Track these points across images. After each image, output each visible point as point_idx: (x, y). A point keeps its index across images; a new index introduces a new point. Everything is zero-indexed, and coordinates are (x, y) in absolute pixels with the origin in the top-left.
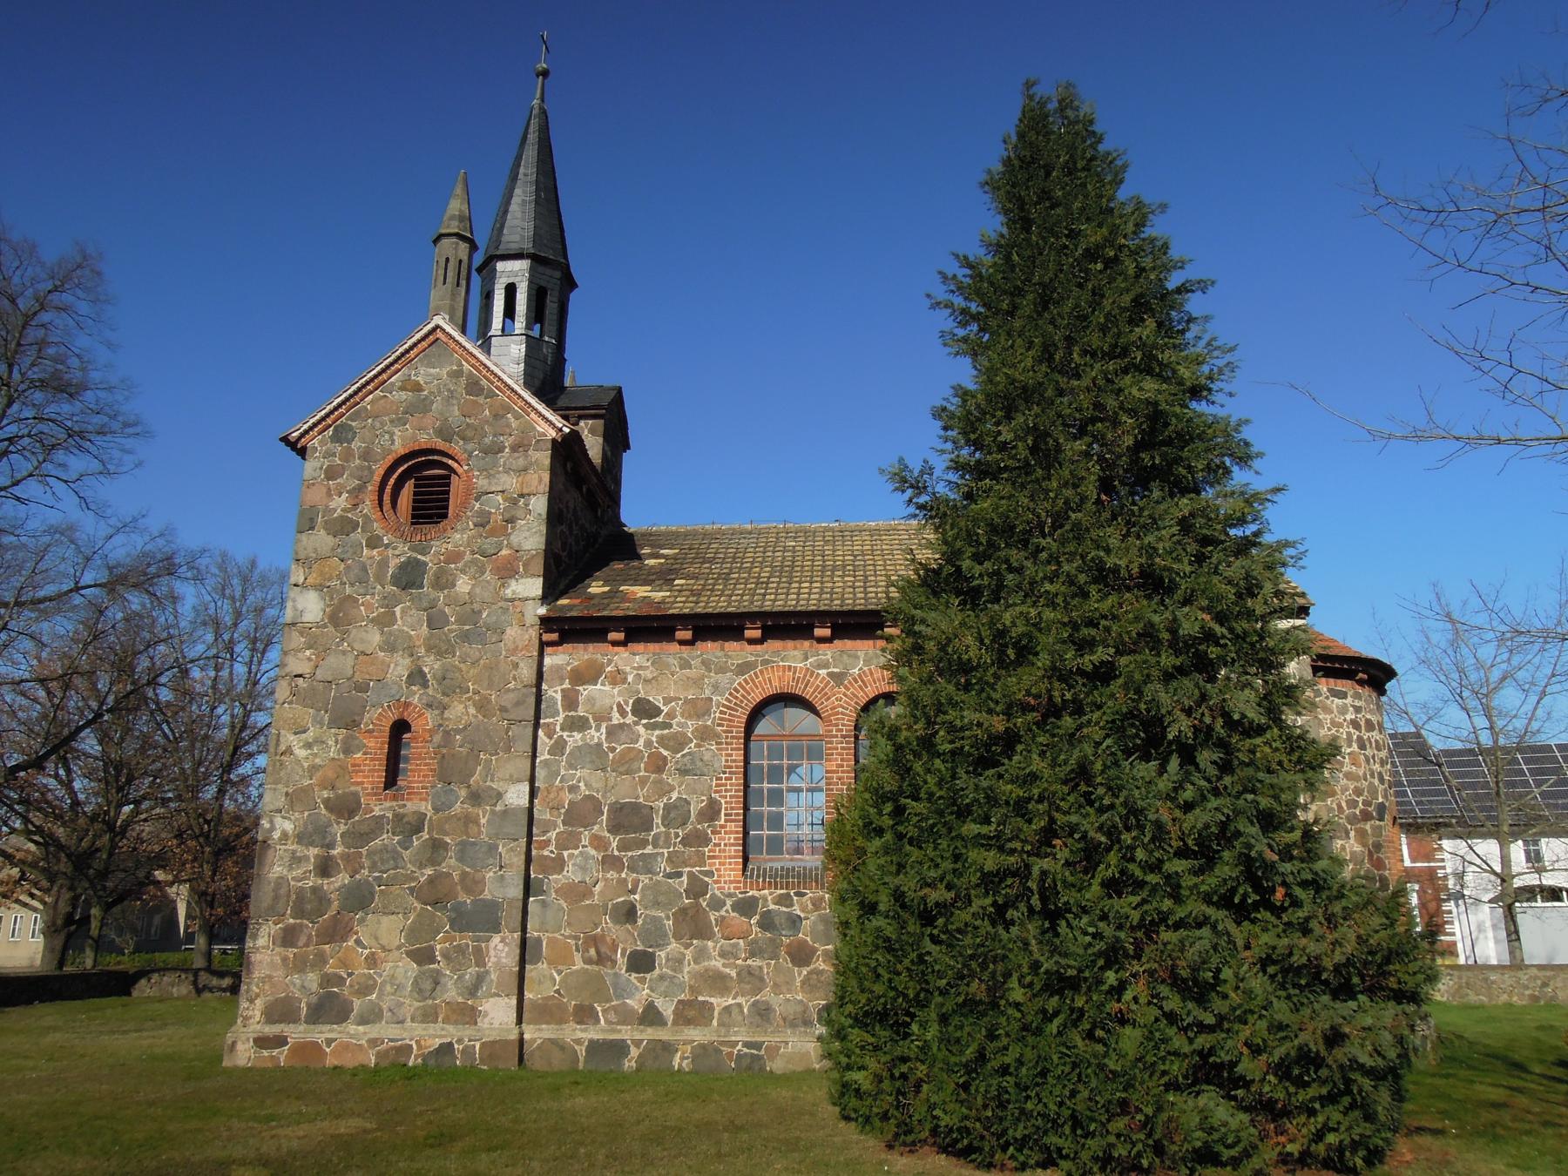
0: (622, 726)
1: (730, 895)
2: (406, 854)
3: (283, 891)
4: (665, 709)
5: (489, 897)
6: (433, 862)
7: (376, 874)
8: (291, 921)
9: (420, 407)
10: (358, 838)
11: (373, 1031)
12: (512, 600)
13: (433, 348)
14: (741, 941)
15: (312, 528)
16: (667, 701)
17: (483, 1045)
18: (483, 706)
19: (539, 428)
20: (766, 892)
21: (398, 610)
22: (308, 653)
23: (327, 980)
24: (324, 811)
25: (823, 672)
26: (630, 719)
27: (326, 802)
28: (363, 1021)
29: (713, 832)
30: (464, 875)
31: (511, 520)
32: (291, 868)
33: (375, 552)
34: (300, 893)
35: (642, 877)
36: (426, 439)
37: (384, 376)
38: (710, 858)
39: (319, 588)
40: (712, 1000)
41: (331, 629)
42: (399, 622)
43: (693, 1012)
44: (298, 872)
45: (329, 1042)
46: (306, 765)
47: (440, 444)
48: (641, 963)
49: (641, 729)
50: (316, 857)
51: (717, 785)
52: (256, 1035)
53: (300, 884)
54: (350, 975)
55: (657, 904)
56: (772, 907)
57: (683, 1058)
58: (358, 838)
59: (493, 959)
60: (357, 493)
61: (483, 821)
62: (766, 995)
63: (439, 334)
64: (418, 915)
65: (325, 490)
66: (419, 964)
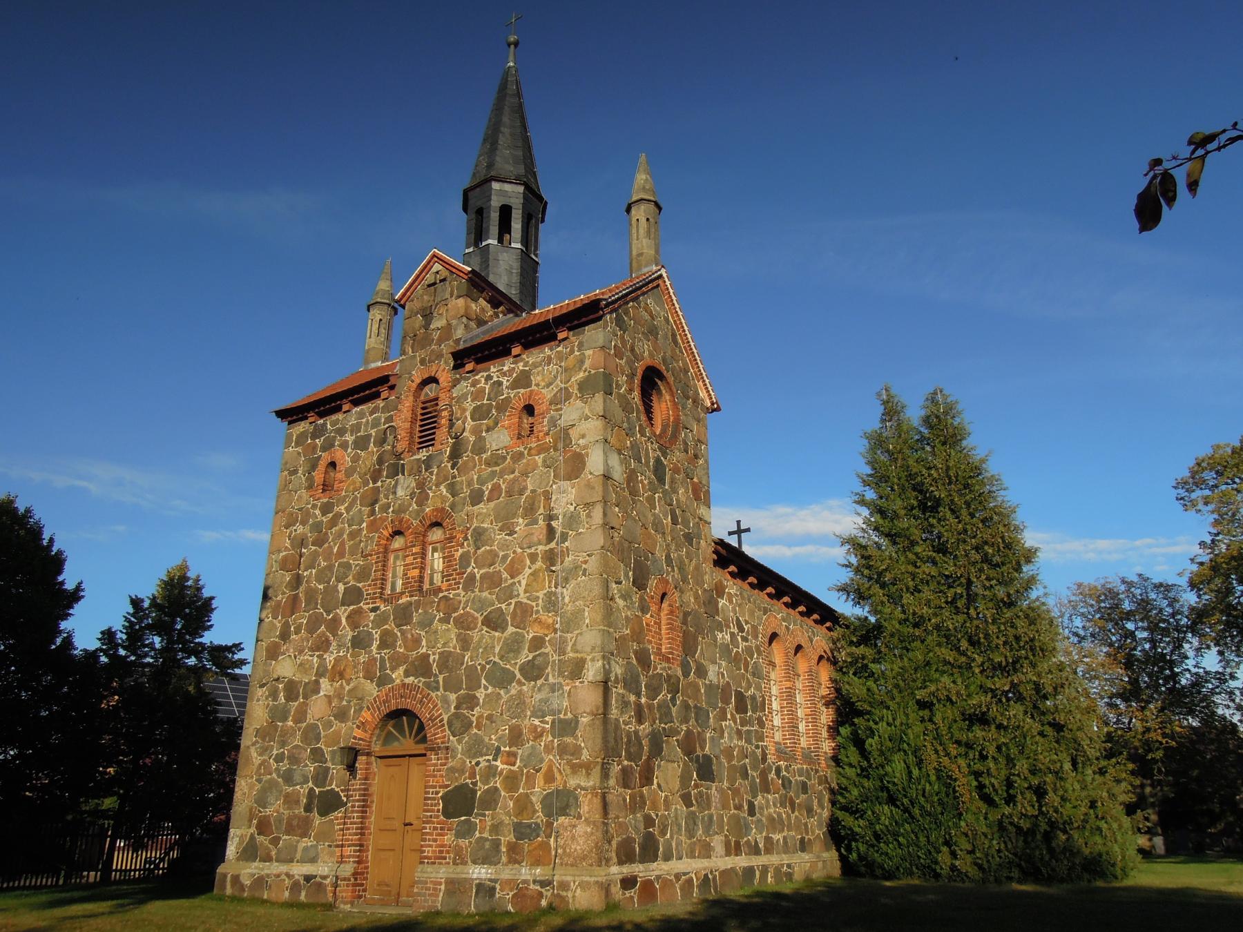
0: (734, 633)
1: (774, 763)
2: (674, 710)
3: (619, 732)
4: (746, 627)
5: (708, 753)
6: (685, 720)
7: (663, 725)
8: (626, 763)
9: (652, 332)
10: (654, 691)
11: (676, 866)
12: (701, 519)
13: (655, 290)
14: (777, 795)
15: (611, 394)
16: (747, 623)
17: (720, 873)
18: (697, 597)
19: (701, 395)
20: (782, 762)
21: (657, 495)
22: (617, 509)
23: (649, 821)
24: (634, 662)
25: (784, 623)
26: (736, 631)
27: (636, 653)
28: (667, 858)
29: (766, 720)
30: (699, 732)
31: (696, 456)
32: (622, 713)
33: (643, 439)
34: (628, 734)
35: (749, 746)
36: (658, 362)
37: (639, 292)
38: (767, 737)
39: (619, 452)
40: (773, 836)
41: (627, 493)
42: (658, 508)
43: (770, 847)
44: (626, 717)
45: (658, 877)
46: (623, 614)
47: (663, 368)
48: (752, 812)
49: (739, 638)
50: (635, 703)
51: (765, 688)
52: (620, 877)
53: (627, 727)
54: (657, 815)
55: (754, 768)
56: (784, 773)
57: (772, 877)
58: (654, 691)
59: (714, 804)
60: (631, 376)
61: (703, 691)
62: (785, 834)
63: (660, 282)
64: (684, 764)
65: (615, 366)
66: (687, 808)
